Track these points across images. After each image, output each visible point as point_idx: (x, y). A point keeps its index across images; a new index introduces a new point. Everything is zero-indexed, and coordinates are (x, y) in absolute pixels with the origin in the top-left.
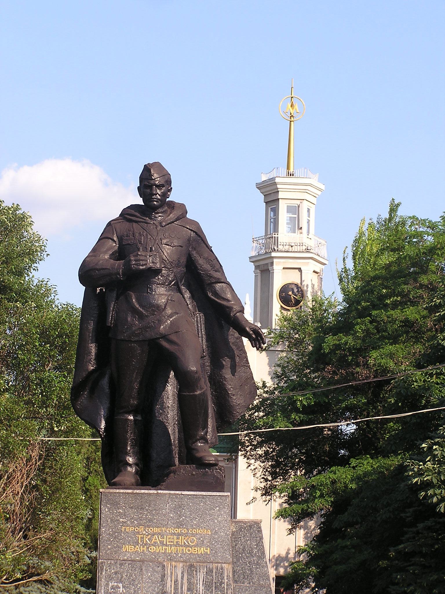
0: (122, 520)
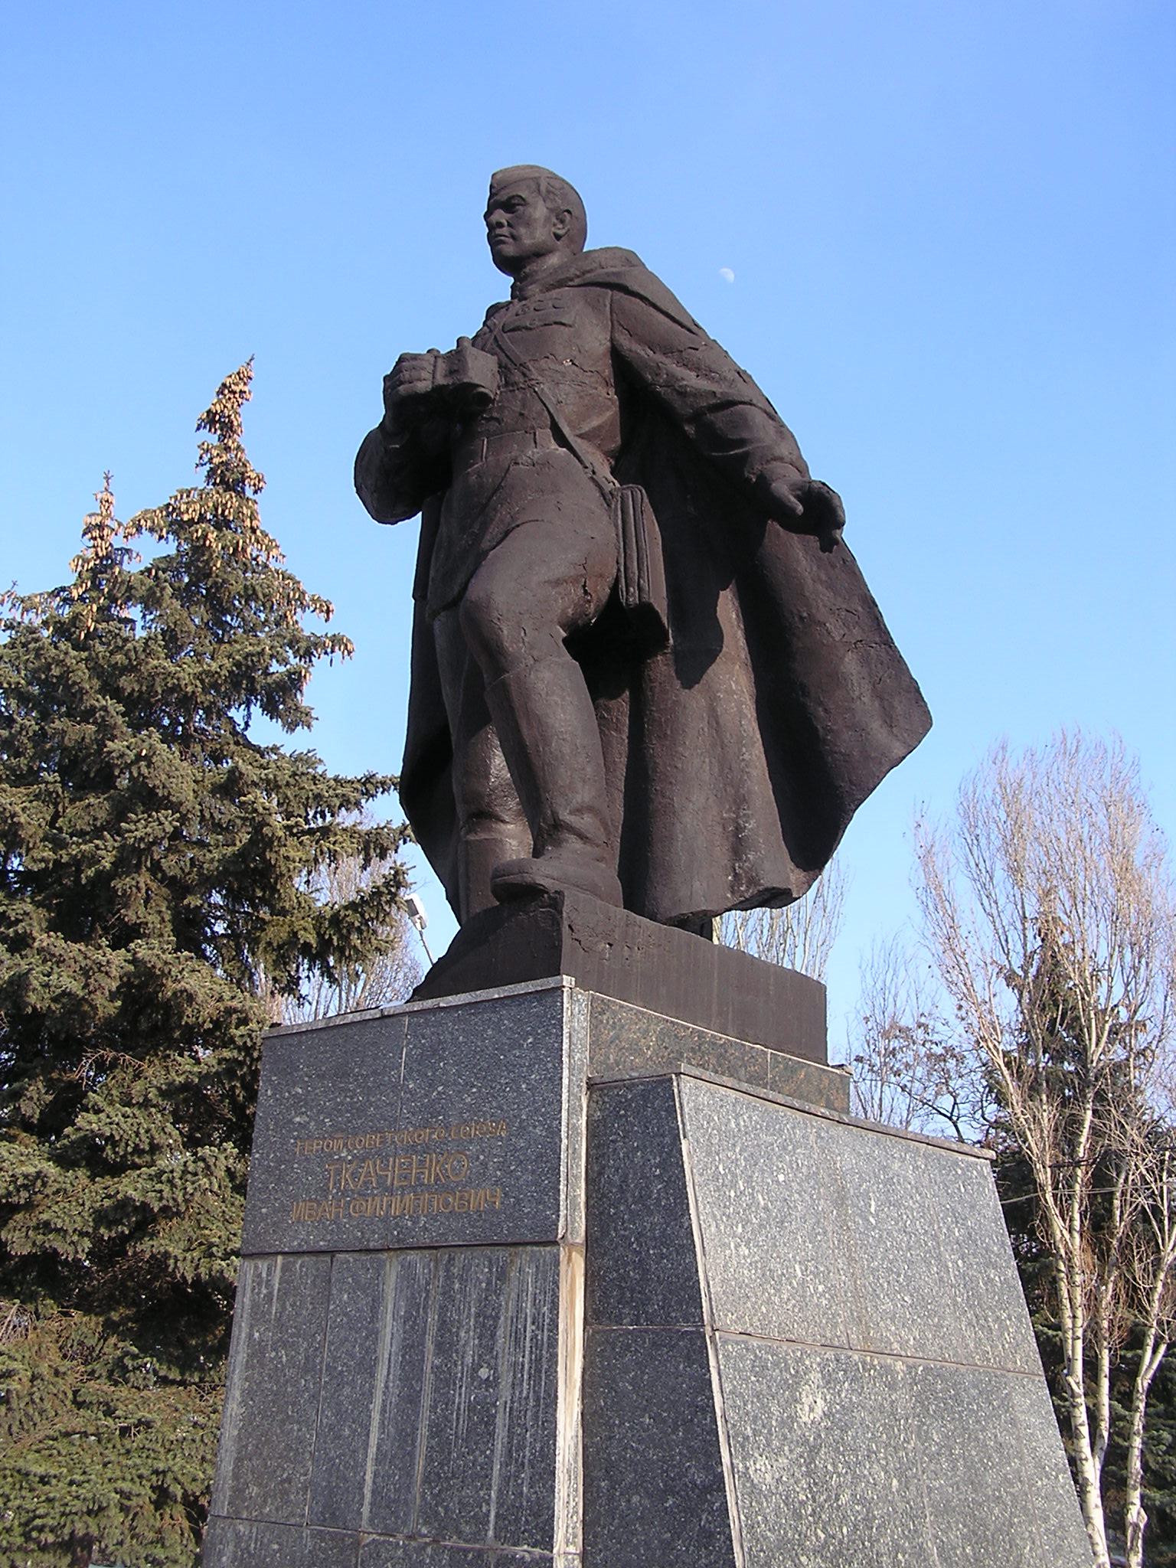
0: (298, 1119)
